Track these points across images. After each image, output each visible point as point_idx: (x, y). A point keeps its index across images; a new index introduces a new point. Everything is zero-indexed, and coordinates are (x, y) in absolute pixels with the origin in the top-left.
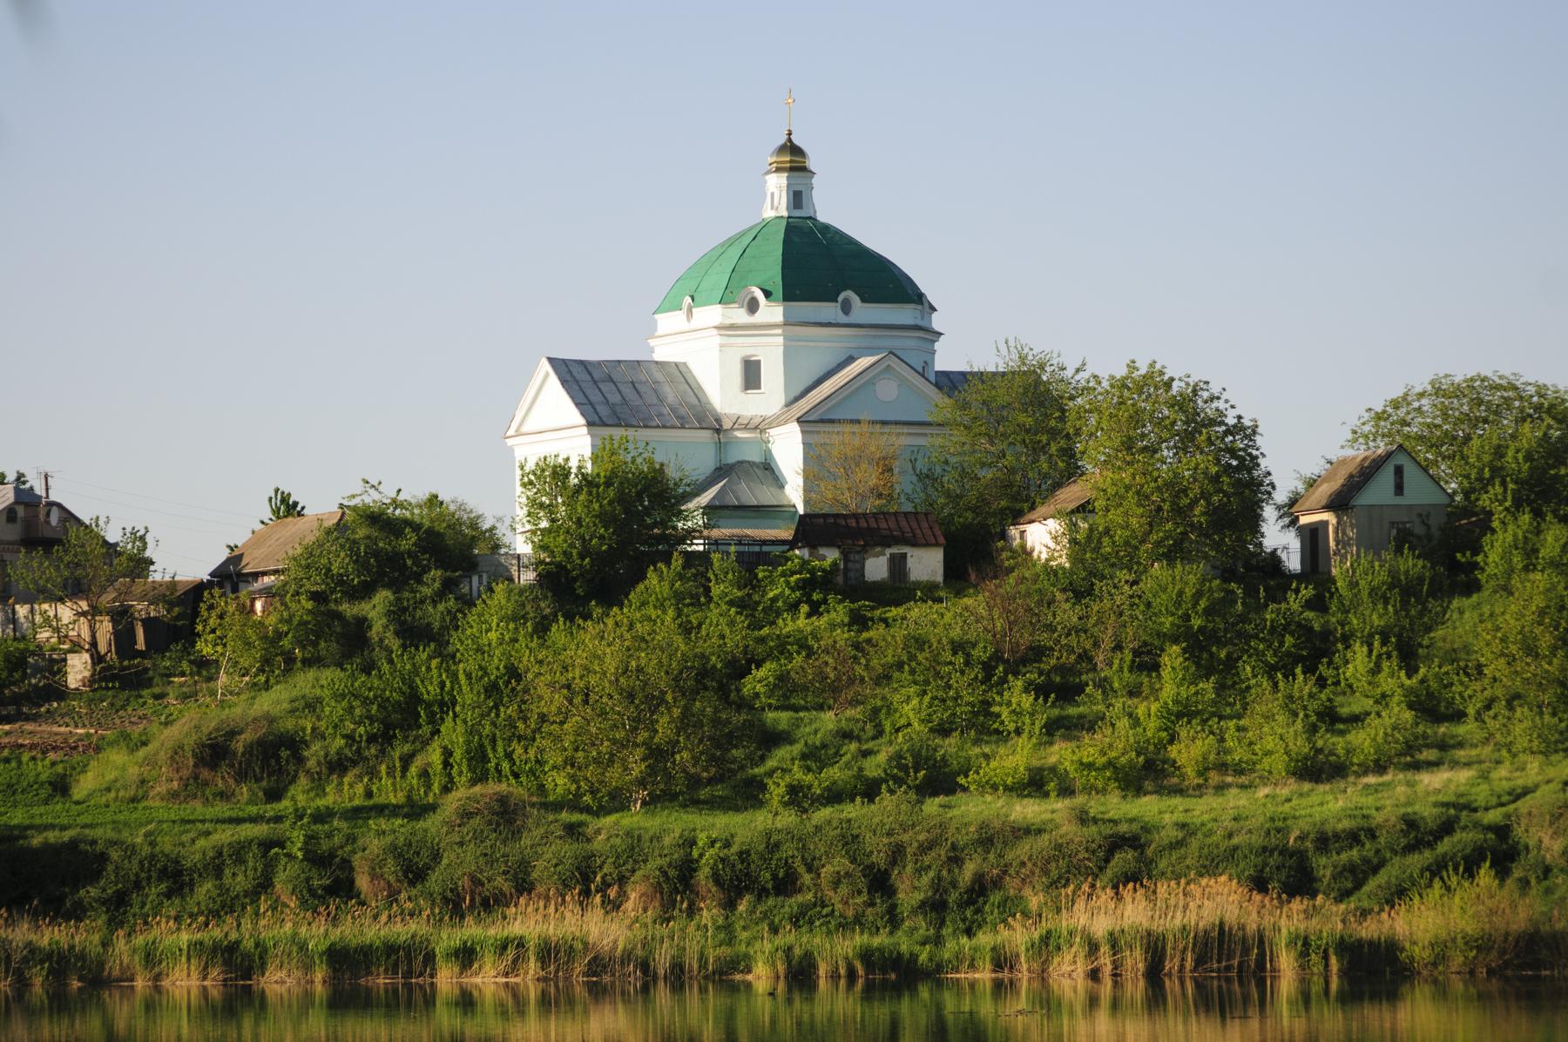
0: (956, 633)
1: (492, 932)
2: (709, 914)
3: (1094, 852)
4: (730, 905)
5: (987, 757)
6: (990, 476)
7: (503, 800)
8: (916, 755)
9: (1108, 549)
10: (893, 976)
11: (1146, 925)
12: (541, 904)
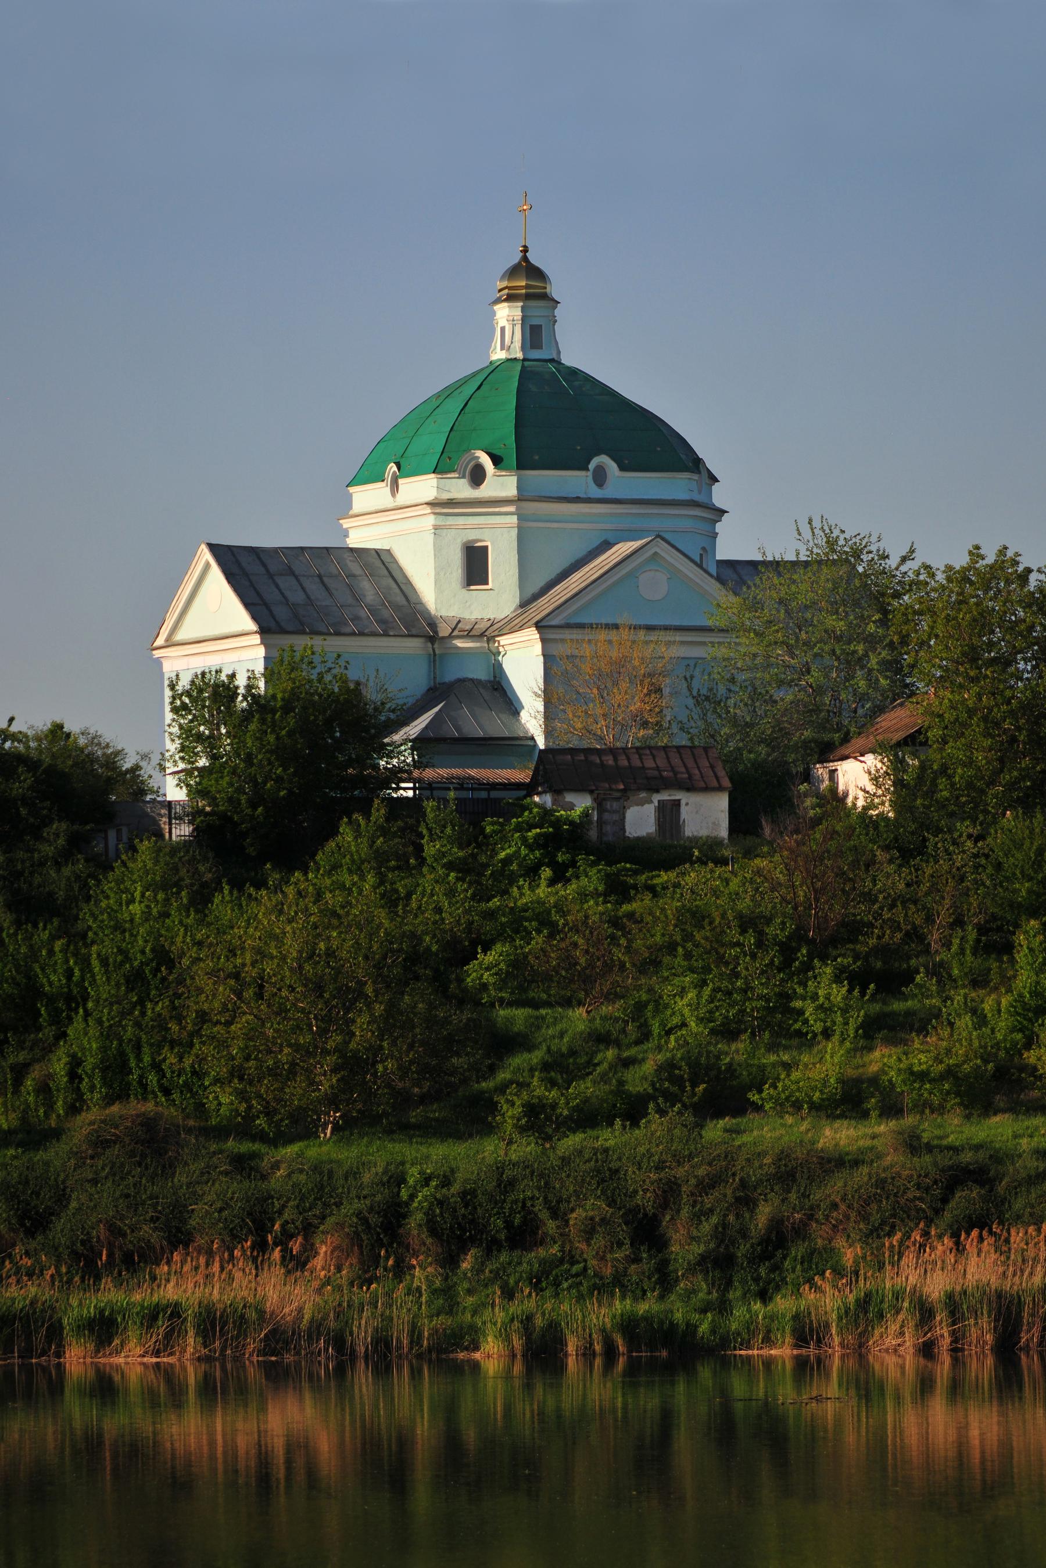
0: (744, 904)
1: (137, 1297)
2: (423, 1274)
3: (927, 1189)
4: (450, 1261)
5: (787, 1067)
6: (790, 697)
7: (149, 1123)
8: (694, 1066)
9: (945, 794)
10: (664, 1354)
11: (995, 1282)
12: (202, 1260)
